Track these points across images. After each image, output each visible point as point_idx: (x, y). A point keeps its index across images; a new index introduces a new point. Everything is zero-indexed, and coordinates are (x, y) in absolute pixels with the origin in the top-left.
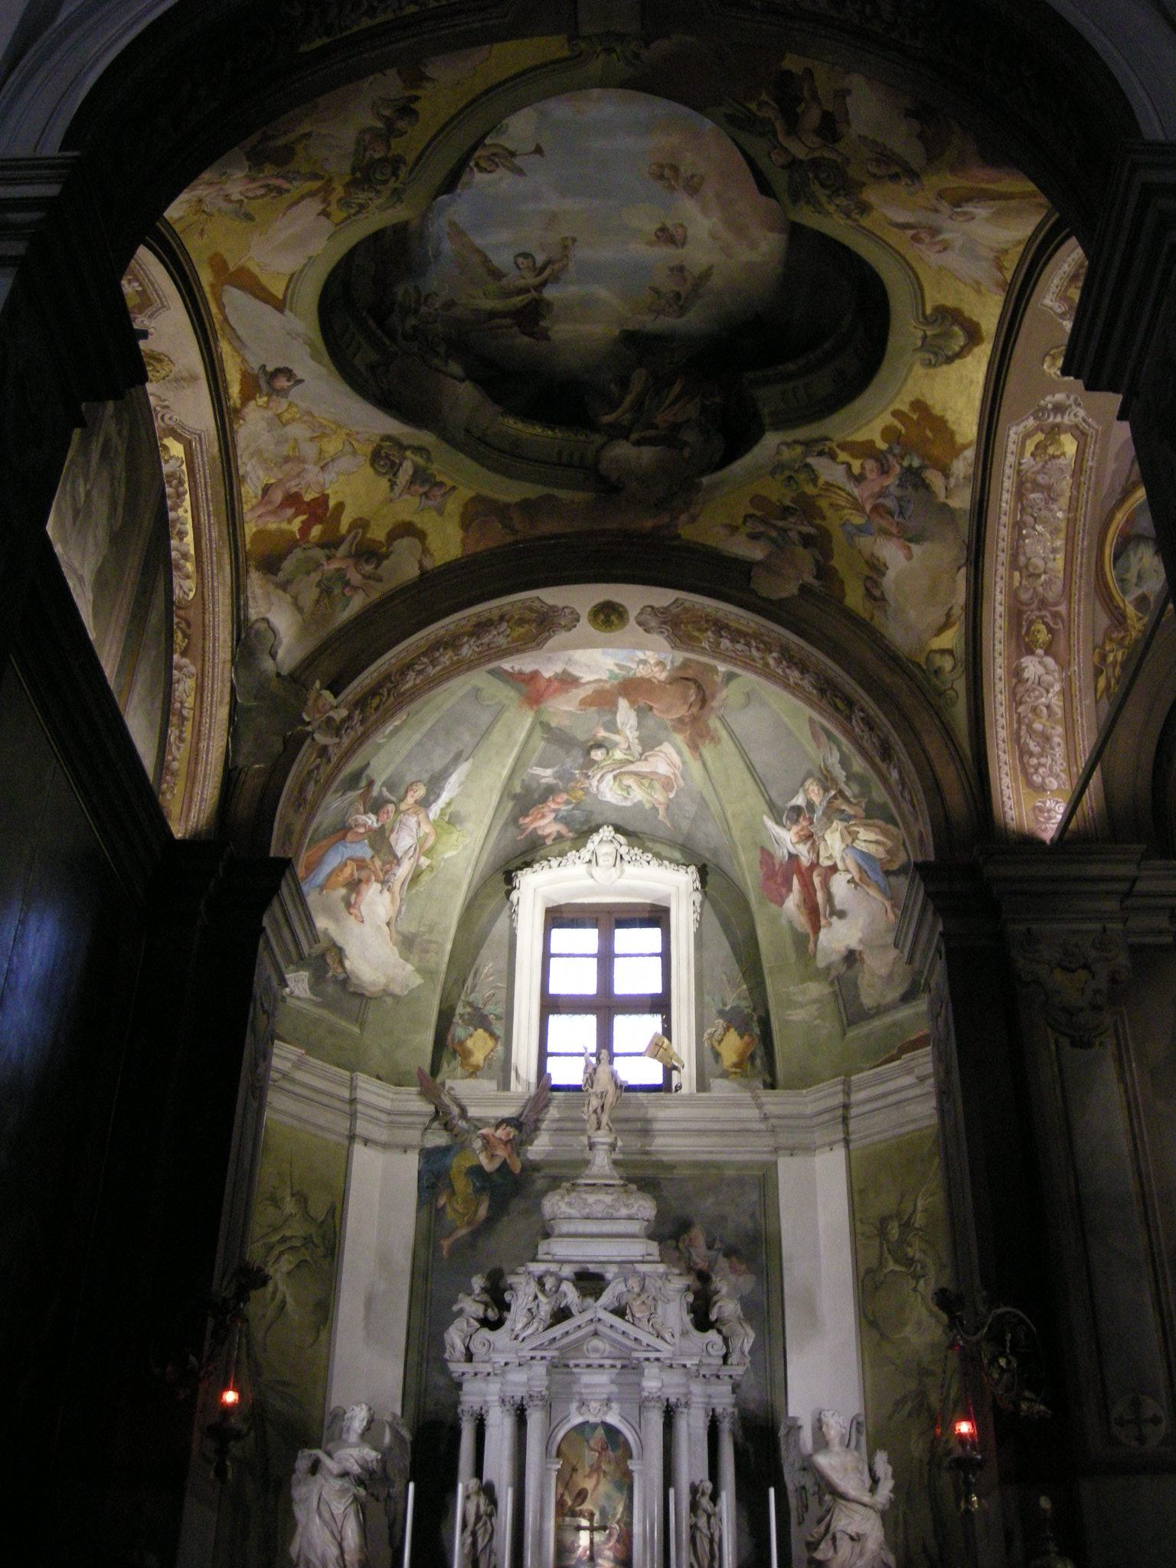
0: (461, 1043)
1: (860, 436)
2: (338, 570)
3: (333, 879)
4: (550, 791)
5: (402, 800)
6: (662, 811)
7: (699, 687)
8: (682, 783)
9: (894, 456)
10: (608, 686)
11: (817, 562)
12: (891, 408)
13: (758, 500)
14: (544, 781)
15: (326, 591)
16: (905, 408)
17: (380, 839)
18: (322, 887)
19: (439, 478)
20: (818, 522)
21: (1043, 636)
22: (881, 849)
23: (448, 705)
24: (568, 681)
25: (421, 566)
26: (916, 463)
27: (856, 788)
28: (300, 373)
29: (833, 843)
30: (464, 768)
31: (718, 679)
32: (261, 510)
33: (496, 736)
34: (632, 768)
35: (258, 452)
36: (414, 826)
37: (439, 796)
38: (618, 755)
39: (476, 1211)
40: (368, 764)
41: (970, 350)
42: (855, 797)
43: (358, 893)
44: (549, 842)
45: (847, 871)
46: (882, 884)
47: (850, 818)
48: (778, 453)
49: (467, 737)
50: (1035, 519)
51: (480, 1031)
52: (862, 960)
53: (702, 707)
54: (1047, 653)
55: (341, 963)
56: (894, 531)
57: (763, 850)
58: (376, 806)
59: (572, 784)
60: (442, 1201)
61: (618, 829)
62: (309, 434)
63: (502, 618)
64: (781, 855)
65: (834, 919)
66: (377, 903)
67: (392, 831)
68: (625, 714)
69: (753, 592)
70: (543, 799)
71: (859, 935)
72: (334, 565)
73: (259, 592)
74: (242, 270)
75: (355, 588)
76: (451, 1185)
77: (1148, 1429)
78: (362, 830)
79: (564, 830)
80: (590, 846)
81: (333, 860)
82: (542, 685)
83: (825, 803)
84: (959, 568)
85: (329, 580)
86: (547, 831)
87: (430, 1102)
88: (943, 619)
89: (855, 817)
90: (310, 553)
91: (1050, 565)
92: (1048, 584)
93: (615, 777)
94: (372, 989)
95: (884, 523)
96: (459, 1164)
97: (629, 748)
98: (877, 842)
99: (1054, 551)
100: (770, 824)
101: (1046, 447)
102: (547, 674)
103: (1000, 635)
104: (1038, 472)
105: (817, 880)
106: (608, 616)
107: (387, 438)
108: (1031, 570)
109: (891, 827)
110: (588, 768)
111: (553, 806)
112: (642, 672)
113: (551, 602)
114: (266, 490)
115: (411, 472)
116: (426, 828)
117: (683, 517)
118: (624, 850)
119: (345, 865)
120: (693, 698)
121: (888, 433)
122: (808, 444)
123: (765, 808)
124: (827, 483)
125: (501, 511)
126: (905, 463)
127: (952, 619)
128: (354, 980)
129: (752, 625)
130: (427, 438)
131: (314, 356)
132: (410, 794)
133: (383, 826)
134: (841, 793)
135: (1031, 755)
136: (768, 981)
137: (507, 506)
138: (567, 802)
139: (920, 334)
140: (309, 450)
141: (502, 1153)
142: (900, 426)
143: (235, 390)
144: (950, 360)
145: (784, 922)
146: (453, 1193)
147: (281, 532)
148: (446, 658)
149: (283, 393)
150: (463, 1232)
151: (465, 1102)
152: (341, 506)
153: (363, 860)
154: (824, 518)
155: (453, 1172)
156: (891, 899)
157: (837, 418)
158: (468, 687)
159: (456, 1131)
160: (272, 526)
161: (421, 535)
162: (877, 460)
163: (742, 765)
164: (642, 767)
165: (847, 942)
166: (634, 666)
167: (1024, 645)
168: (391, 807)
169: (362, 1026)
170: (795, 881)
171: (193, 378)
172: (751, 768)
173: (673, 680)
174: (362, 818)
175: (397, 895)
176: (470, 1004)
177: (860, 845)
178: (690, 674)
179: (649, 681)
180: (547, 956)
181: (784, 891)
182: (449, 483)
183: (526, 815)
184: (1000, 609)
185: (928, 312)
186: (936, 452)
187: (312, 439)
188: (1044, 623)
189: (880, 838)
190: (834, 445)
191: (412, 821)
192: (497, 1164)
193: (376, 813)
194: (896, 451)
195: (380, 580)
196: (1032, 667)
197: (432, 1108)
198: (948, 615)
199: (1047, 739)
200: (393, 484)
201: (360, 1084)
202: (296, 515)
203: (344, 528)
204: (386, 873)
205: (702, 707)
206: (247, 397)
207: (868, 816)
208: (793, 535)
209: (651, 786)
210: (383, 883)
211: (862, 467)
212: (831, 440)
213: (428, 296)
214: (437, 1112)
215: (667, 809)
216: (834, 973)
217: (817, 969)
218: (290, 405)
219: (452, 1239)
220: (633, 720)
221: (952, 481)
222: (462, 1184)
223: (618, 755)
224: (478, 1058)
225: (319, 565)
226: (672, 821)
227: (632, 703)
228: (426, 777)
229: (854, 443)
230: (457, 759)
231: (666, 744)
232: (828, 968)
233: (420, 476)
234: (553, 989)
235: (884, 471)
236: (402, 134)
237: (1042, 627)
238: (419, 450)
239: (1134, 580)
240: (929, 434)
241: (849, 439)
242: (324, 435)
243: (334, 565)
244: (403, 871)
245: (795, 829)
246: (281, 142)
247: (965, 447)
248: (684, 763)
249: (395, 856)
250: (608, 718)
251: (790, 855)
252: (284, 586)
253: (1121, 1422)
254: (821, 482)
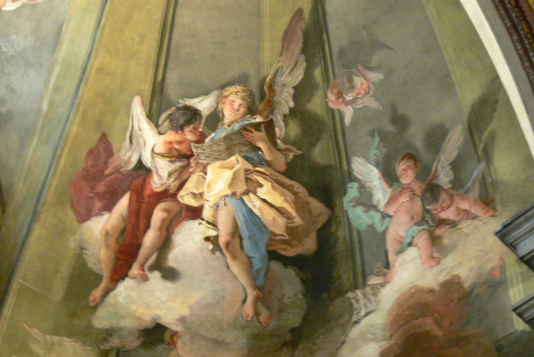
22: (281, 221)
27: (294, 130)
29: (216, 182)
42: (285, 141)
45: (214, 225)
46: (257, 264)
47: (263, 162)
52: (172, 344)
57: (104, 137)
64: (127, 157)
65: (157, 274)
71: (186, 312)
83: (237, 127)
89: (269, 164)
98: (280, 211)
100: (138, 110)
105: (158, 215)
109: (316, 205)
123: (147, 88)
134: (269, 126)
136: (11, 301)
145: (72, 244)
156: (259, 288)
163: (158, 16)
165: (157, 312)
170: (123, 203)
172: (167, 27)
177: (253, 202)
181: (98, 204)
189: (290, 209)
207: (292, 171)
216: (115, 342)
217: (90, 326)
232: (109, 333)
245: (171, 136)
251: (140, 162)
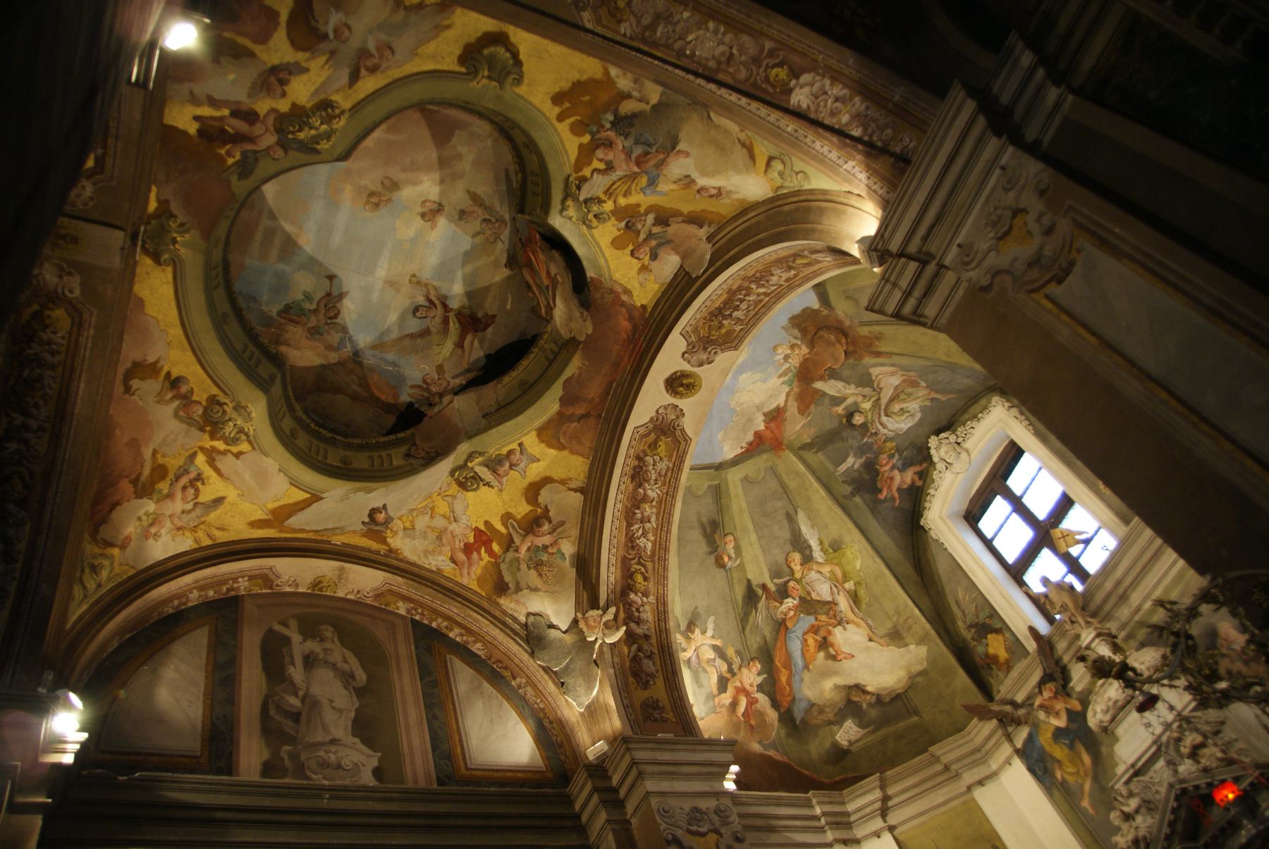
0: (987, 655)
1: (573, 153)
2: (529, 549)
3: (808, 656)
4: (871, 468)
5: (792, 572)
6: (934, 395)
7: (828, 328)
8: (912, 374)
9: (599, 132)
10: (796, 390)
11: (683, 221)
12: (555, 122)
13: (617, 244)
14: (856, 466)
15: (538, 565)
16: (557, 110)
17: (808, 605)
18: (806, 667)
19: (504, 451)
20: (642, 210)
21: (782, 73)
23: (744, 504)
24: (775, 416)
25: (575, 490)
26: (610, 117)
28: (379, 504)
30: (802, 518)
31: (825, 312)
32: (465, 571)
33: (792, 484)
34: (884, 401)
35: (426, 553)
36: (819, 576)
37: (810, 547)
38: (867, 406)
39: (1082, 761)
40: (749, 581)
41: (513, 45)
43: (832, 645)
44: (919, 483)
48: (570, 218)
49: (779, 504)
50: (680, 38)
51: (989, 636)
53: (846, 335)
54: (797, 77)
55: (865, 692)
56: (662, 156)
58: (783, 593)
59: (875, 447)
60: (1059, 775)
61: (937, 433)
62: (427, 517)
63: (639, 458)
66: (849, 637)
67: (809, 594)
68: (830, 387)
69: (698, 278)
70: (877, 473)
72: (523, 550)
73: (512, 605)
74: (274, 512)
75: (555, 543)
76: (1054, 758)
78: (792, 613)
79: (917, 468)
80: (935, 459)
81: (795, 646)
82: (768, 434)
84: (709, 117)
85: (531, 559)
86: (908, 480)
87: (991, 719)
88: (745, 151)
90: (507, 560)
92: (742, 50)
93: (887, 415)
94: (901, 685)
95: (653, 162)
96: (1045, 739)
97: (864, 396)
99: (716, 32)
101: (617, 8)
102: (762, 427)
104: (639, 22)
106: (682, 385)
107: (452, 473)
108: (723, 59)
110: (867, 430)
111: (887, 468)
112: (795, 362)
113: (647, 419)
114: (453, 560)
115: (485, 469)
116: (826, 570)
117: (624, 298)
118: (952, 438)
119: (806, 640)
120: (832, 337)
121: (577, 130)
122: (567, 195)
124: (605, 193)
125: (561, 418)
126: (608, 126)
127: (748, 143)
128: (884, 693)
129: (719, 292)
130: (464, 448)
131: (369, 491)
132: (792, 565)
133: (801, 598)
137: (560, 414)
138: (891, 457)
139: (485, 81)
140: (439, 522)
141: (1060, 706)
142: (573, 119)
143: (374, 545)
144: (518, 63)
146: (1059, 762)
147: (485, 567)
148: (648, 510)
149: (389, 520)
150: (1087, 786)
151: (1009, 697)
152: (487, 523)
153: (813, 626)
154: (638, 205)
155: (1047, 748)
157: (552, 166)
158: (739, 484)
159: (1023, 719)
160: (479, 571)
161: (547, 480)
162: (598, 147)
164: (886, 395)
166: (787, 365)
168: (792, 584)
169: (916, 713)
171: (342, 569)
173: (811, 344)
174: (784, 608)
175: (856, 619)
176: (971, 626)
178: (812, 329)
179: (806, 360)
180: (988, 544)
182: (514, 446)
183: (880, 491)
185: (463, 70)
186: (604, 97)
187: (432, 517)
188: (773, 67)
190: (574, 175)
191: (813, 575)
192: (1064, 716)
193: (788, 596)
194: (595, 129)
195: (562, 523)
197: (995, 721)
198: (743, 145)
200: (488, 484)
201: (939, 753)
202: (479, 553)
203: (503, 530)
204: (835, 616)
205: (846, 335)
206: (383, 541)
208: (656, 230)
209: (910, 395)
210: (839, 624)
211: (601, 160)
212: (569, 176)
213: (424, 381)
214: (1000, 721)
215: (936, 391)
218: (400, 519)
219: (1086, 795)
220: (840, 385)
221: (635, 93)
222: (1059, 752)
223: (867, 406)
224: (1003, 655)
225: (517, 559)
226: (950, 392)
227: (822, 378)
228: (788, 547)
229: (577, 160)
230: (791, 519)
231: (871, 370)
233: (494, 464)
234: (1011, 557)
235: (609, 145)
236: (191, 391)
237: (775, 71)
238: (470, 457)
240: (587, 98)
241: (573, 162)
242: (432, 509)
243: (523, 550)
244: (843, 604)
246: (146, 472)
247: (607, 73)
248: (893, 365)
249: (829, 603)
250: (827, 401)
252: (519, 589)
254: (603, 197)
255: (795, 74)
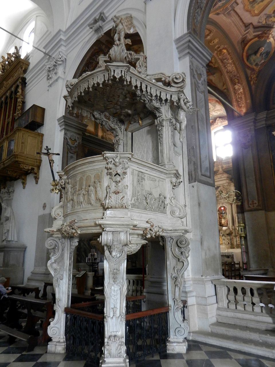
21: (237, 81)
34: (215, 110)
77: (255, 205)
91: (233, 69)
103: (230, 84)
135: (239, 102)
167: (234, 84)
184: (228, 80)
196: (237, 87)
198: (223, 83)
199: (241, 98)
239: (253, 62)
253: (251, 204)
255: (238, 83)
